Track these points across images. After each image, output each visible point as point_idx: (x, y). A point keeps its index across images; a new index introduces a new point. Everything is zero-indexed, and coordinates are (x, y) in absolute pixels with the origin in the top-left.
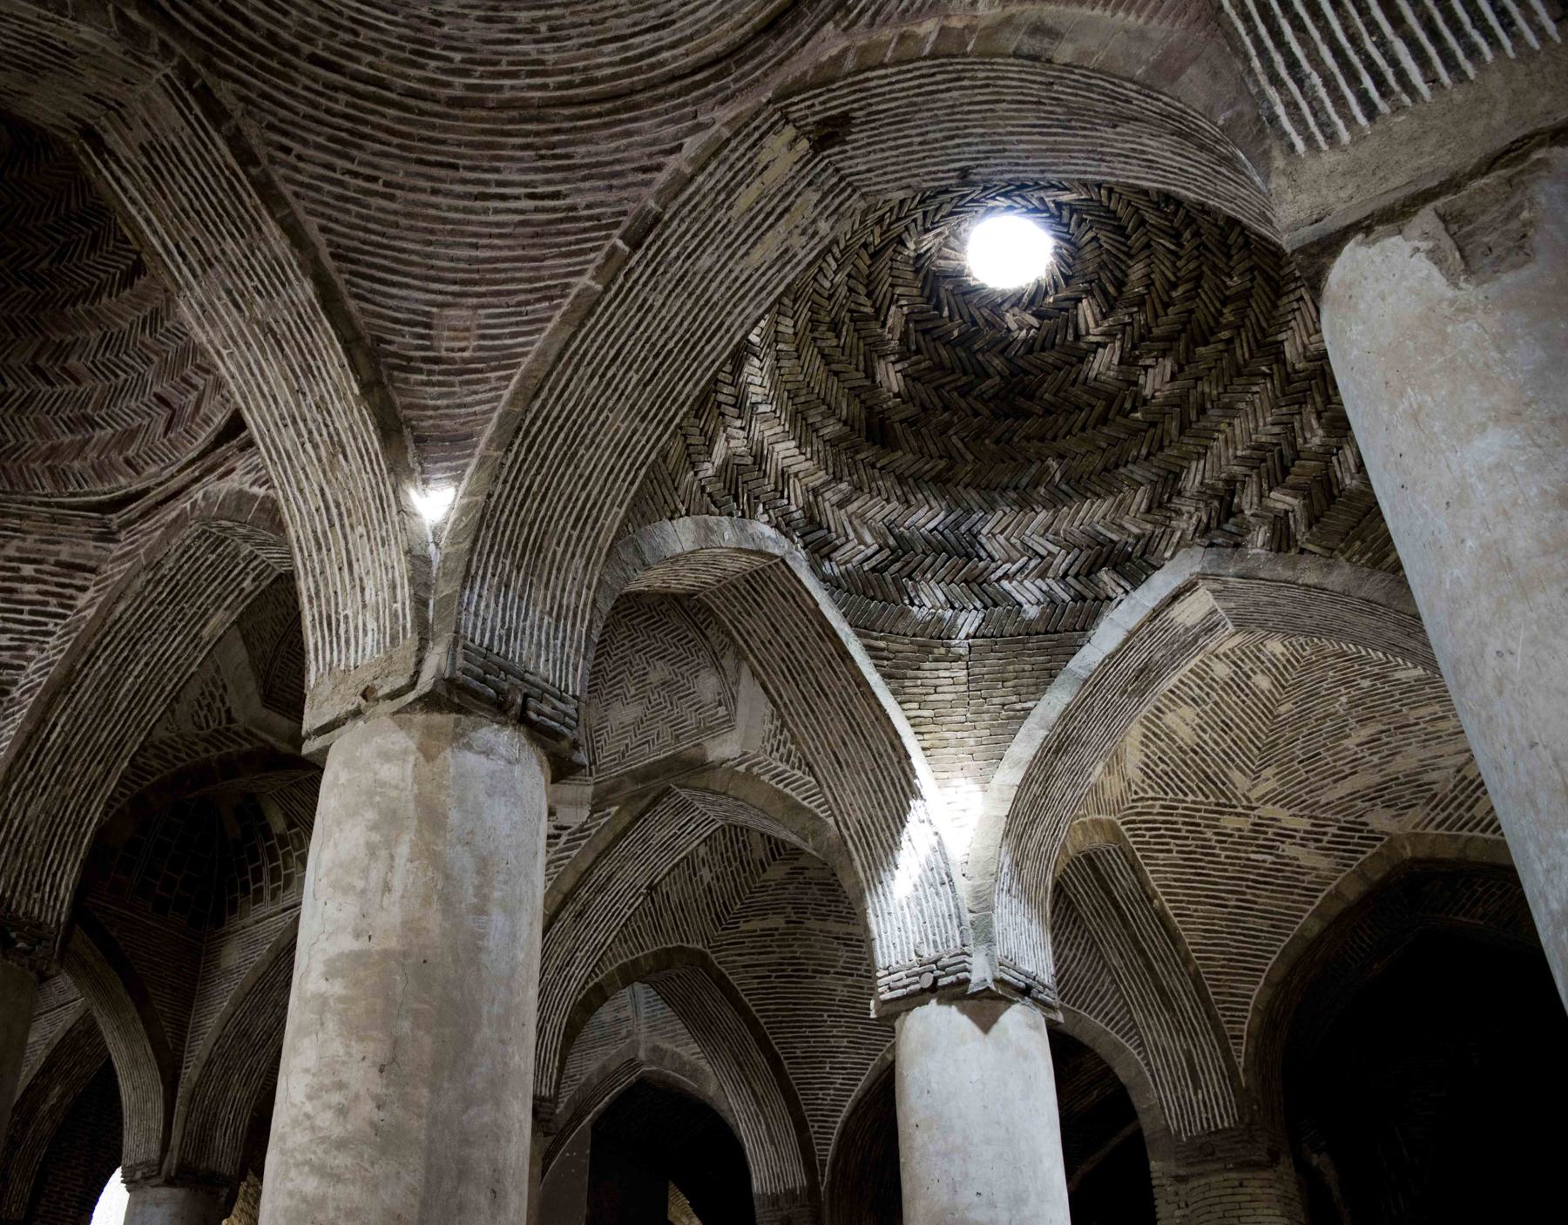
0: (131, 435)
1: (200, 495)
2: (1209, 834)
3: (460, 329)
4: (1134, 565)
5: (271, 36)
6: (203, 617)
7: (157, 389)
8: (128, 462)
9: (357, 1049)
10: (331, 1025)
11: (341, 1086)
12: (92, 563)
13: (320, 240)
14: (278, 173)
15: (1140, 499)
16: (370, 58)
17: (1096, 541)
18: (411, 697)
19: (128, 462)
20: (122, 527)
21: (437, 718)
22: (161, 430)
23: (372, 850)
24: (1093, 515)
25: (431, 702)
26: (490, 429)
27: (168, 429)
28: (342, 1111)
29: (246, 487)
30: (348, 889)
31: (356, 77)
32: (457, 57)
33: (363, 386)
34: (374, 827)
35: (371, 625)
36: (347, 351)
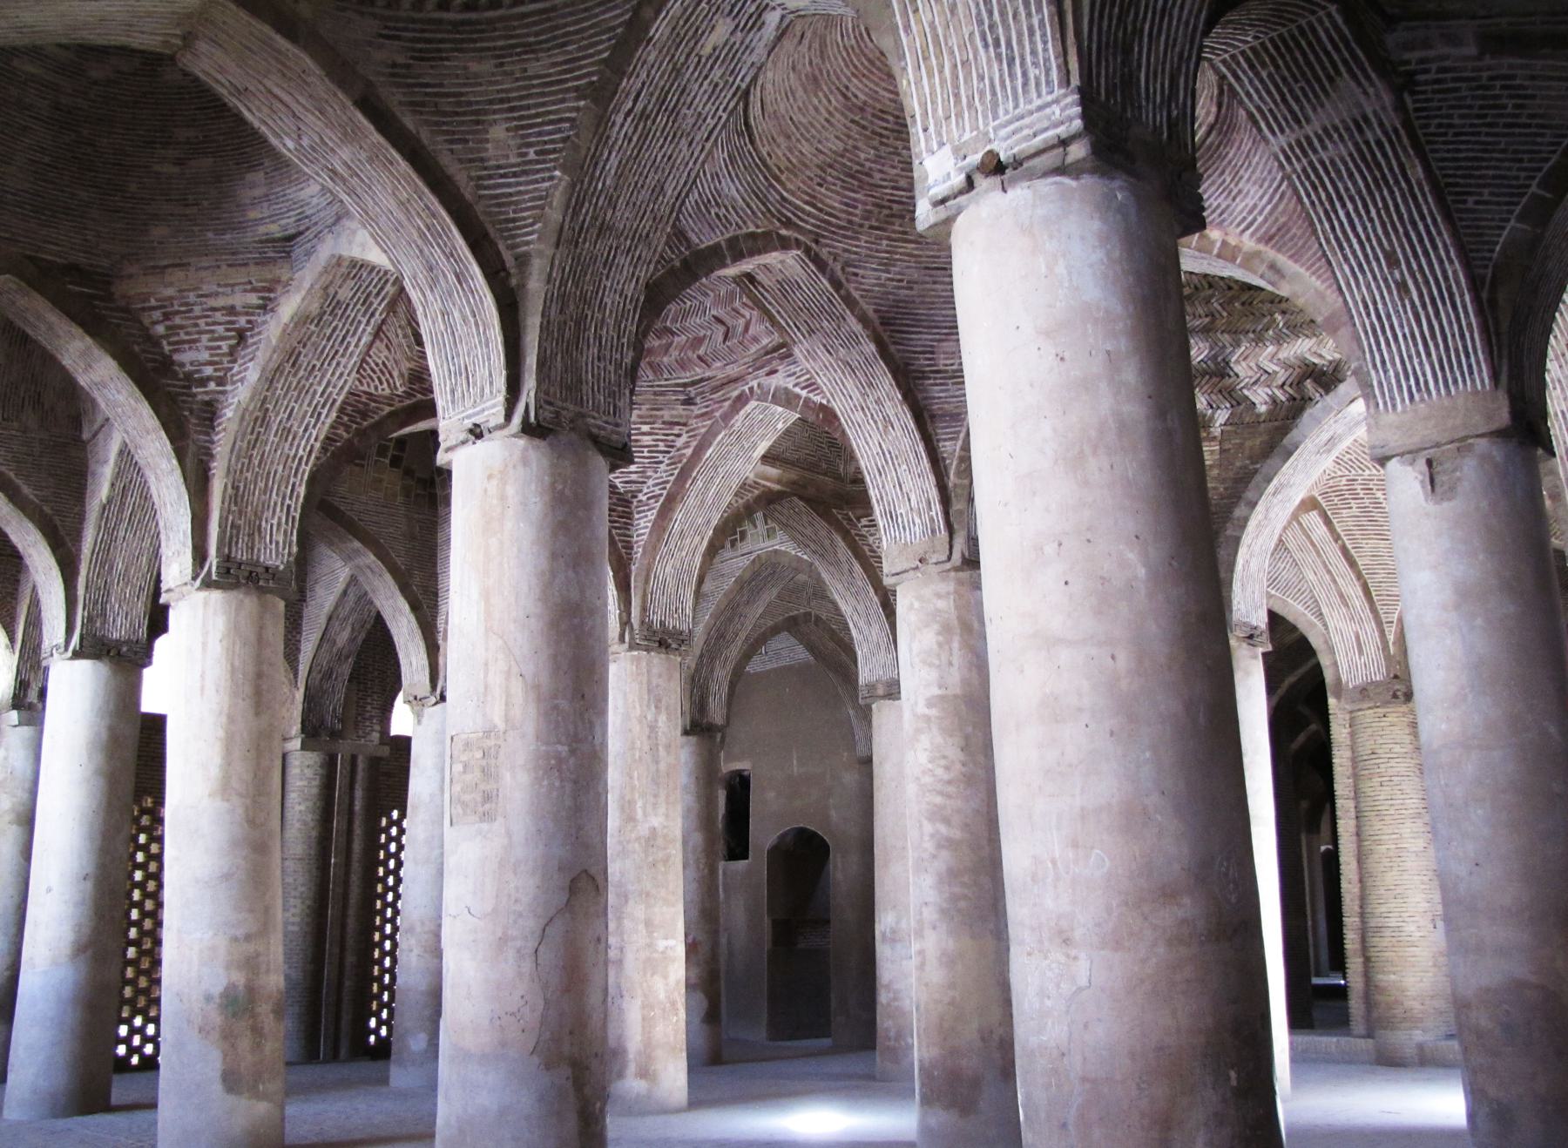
0: (699, 341)
1: (755, 383)
6: (754, 446)
7: (714, 312)
8: (699, 357)
10: (935, 730)
11: (944, 757)
12: (682, 420)
14: (851, 287)
18: (948, 566)
21: (961, 574)
22: (721, 339)
23: (940, 645)
27: (726, 338)
28: (947, 768)
29: (790, 386)
30: (931, 665)
33: (905, 396)
34: (939, 633)
35: (917, 521)
36: (895, 377)
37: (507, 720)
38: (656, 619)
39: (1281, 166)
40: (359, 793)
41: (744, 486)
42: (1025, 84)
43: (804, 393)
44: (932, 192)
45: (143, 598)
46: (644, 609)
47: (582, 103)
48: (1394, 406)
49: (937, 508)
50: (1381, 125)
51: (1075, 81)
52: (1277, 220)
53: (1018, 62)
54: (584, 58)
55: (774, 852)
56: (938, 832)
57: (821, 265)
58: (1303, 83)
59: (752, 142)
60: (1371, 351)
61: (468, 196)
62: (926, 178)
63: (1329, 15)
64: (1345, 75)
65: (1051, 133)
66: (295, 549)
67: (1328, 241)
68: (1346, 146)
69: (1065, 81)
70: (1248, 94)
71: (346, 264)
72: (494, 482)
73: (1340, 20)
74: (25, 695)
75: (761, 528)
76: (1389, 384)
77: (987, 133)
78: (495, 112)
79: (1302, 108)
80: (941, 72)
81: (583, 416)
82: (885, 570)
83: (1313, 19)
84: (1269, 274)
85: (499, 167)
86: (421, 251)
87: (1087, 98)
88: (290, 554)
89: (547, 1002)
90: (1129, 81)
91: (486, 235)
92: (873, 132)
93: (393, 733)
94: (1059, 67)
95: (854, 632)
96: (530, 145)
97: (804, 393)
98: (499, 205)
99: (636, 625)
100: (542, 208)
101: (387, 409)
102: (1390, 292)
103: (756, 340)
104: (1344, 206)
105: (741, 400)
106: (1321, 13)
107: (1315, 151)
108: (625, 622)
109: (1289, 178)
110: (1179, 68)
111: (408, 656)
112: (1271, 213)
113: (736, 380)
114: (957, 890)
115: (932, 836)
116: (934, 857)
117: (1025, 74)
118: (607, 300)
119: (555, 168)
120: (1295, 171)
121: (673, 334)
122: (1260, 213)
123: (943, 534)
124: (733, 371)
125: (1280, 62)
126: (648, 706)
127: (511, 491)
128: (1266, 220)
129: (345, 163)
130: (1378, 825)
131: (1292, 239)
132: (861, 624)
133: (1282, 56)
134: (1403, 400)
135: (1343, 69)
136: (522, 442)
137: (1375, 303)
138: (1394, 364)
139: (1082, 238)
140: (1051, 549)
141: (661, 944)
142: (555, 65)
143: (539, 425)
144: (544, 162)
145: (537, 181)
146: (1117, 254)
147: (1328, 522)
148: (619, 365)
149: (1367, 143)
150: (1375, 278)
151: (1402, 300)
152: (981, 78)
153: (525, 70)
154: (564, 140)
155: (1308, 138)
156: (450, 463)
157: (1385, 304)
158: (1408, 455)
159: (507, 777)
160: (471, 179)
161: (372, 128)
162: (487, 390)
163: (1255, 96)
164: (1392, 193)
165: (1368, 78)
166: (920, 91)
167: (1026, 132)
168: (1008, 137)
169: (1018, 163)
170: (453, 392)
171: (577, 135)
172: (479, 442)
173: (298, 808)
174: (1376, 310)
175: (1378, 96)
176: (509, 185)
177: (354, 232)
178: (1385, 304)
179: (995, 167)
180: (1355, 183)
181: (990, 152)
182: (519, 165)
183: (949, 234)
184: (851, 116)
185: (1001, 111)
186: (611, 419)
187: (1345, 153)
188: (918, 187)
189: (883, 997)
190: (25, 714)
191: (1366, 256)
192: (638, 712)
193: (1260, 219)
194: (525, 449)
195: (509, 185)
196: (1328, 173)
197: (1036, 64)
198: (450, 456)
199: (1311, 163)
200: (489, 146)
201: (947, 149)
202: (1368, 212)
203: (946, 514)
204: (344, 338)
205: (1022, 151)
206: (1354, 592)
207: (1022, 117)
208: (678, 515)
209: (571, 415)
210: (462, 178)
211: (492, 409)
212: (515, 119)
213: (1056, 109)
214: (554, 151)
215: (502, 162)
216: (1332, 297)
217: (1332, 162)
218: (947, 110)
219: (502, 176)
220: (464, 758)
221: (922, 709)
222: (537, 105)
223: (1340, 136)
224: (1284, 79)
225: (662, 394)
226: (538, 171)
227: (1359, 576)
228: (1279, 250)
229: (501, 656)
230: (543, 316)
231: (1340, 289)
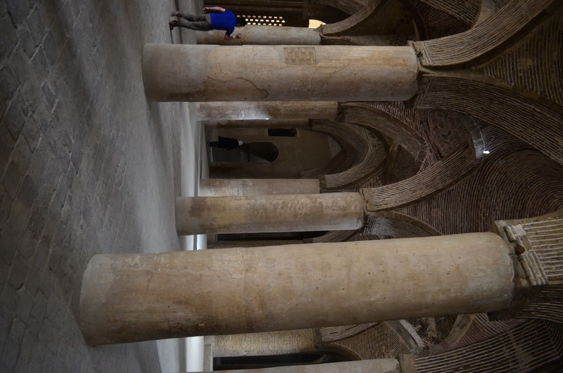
0: (442, 126)
1: (427, 145)
2: (382, 343)
3: (437, 213)
4: (422, 332)
5: (485, 182)
6: (405, 144)
8: (437, 126)
9: (308, 209)
10: (312, 204)
11: (303, 207)
13: (451, 188)
14: (462, 181)
15: (435, 335)
16: (485, 198)
17: (427, 325)
18: (365, 210)
19: (437, 126)
20: (424, 126)
21: (363, 214)
23: (339, 207)
24: (432, 324)
25: (364, 213)
26: (417, 219)
27: (443, 135)
28: (299, 208)
30: (333, 204)
31: (481, 197)
32: (487, 215)
33: (423, 197)
35: (381, 200)
36: (429, 194)
37: (320, 67)
38: (348, 111)
39: (502, 333)
40: (290, 9)
41: (391, 139)
42: (549, 264)
43: (424, 162)
44: (509, 227)
46: (351, 107)
47: (539, 93)
48: (416, 364)
49: (385, 207)
50: (515, 369)
51: (551, 283)
52: (481, 328)
53: (558, 261)
54: (556, 95)
55: (270, 145)
56: (279, 205)
57: (470, 172)
58: (531, 344)
59: (517, 151)
60: (435, 357)
61: (506, 51)
62: (514, 225)
63: (556, 356)
64: (534, 359)
65: (531, 273)
67: (474, 346)
68: (508, 356)
69: (550, 279)
70: (528, 325)
71: (478, 5)
72: (402, 62)
73: (554, 359)
75: (376, 143)
76: (424, 363)
77: (531, 248)
78: (537, 61)
79: (522, 343)
80: (554, 232)
81: (424, 93)
82: (365, 189)
83: (555, 350)
84: (462, 324)
85: (516, 63)
86: (486, 34)
87: (543, 287)
89: (225, 82)
90: (547, 299)
91: (491, 58)
92: (517, 191)
93: (311, 21)
94: (556, 277)
95: (342, 173)
96: (524, 75)
97: (424, 162)
98: (502, 62)
99: (346, 104)
100: (500, 78)
101: (423, 19)
102: (455, 365)
103: (442, 146)
104: (486, 353)
105: (422, 140)
106: (557, 353)
107: (506, 345)
109: (496, 336)
110: (549, 315)
111: (336, 26)
112: (483, 326)
113: (429, 138)
114: (260, 211)
115: (278, 203)
116: (271, 204)
117: (553, 264)
118: (465, 101)
119: (515, 83)
120: (499, 338)
121: (445, 118)
122: (483, 322)
123: (376, 209)
124: (432, 137)
125: (539, 337)
127: (399, 68)
128: (481, 324)
129: (520, 6)
130: (277, 336)
131: (474, 333)
132: (344, 176)
133: (542, 338)
134: (418, 367)
135: (536, 358)
136: (416, 71)
137: (452, 360)
138: (430, 365)
139: (491, 282)
140: (381, 267)
141: (243, 112)
142: (554, 83)
143: (422, 77)
144: (517, 79)
145: (510, 76)
146: (485, 294)
147: (373, 327)
148: (441, 105)
149: (508, 363)
150: (460, 361)
151: (452, 369)
152: (552, 247)
153: (552, 72)
154: (525, 87)
155: (511, 343)
156: (409, 45)
157: (451, 363)
158: (400, 368)
159: (300, 68)
160: (513, 52)
161: (534, 16)
162: (434, 59)
163: (527, 327)
164: (490, 369)
165: (532, 366)
166: (547, 223)
167: (532, 263)
168: (530, 257)
169: (520, 260)
170: (434, 46)
171: (527, 91)
172: (415, 56)
174: (449, 360)
175: (524, 369)
176: (509, 66)
177: (490, 8)
178: (451, 363)
179: (518, 251)
180: (494, 357)
181: (524, 250)
182: (517, 70)
183: (493, 232)
184: (524, 184)
185: (539, 254)
186: (422, 102)
187: (505, 355)
188: (510, 221)
189: (226, 181)
191: (468, 359)
193: (481, 322)
194: (413, 73)
195: (509, 66)
196: (498, 349)
197: (557, 268)
198: (411, 45)
199: (502, 343)
200: (525, 59)
201: (525, 233)
202: (483, 361)
203: (383, 210)
204: (451, 4)
205: (524, 262)
206: (350, 333)
207: (537, 262)
208: (383, 119)
209: (424, 88)
210: (514, 49)
211: (427, 61)
212: (534, 69)
213: (540, 275)
214: (521, 83)
215: (518, 64)
216: (453, 345)
217: (502, 351)
218: (540, 233)
219: (513, 64)
220: (307, 52)
221: (319, 200)
222: (539, 76)
223: (511, 354)
224: (533, 338)
225: (424, 113)
226: (514, 77)
227: (355, 335)
228: (470, 327)
229: (342, 65)
230: (461, 79)
231: (457, 349)
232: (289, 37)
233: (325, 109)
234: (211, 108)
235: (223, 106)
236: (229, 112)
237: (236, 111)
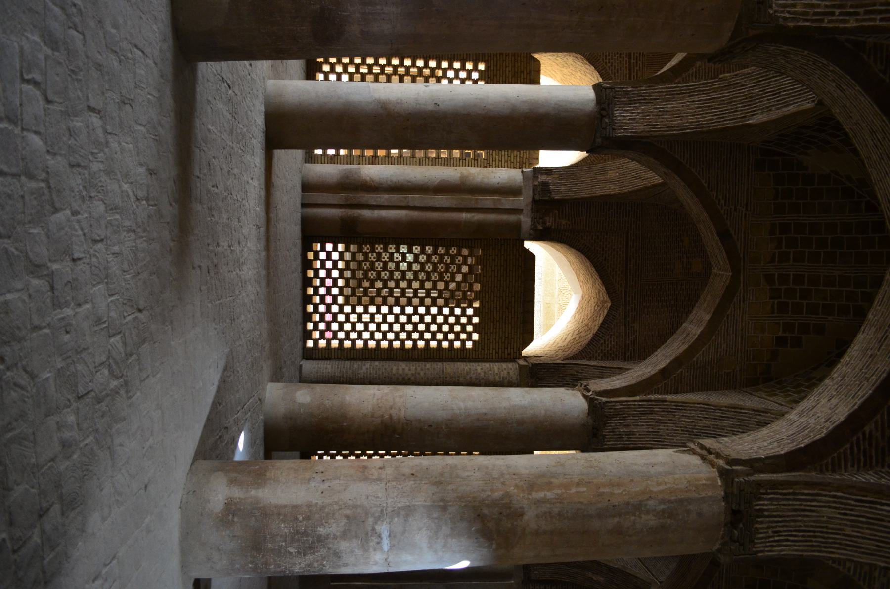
45: (647, 129)
46: (774, 485)
66: (791, 24)
74: (542, 174)
88: (785, 19)
108: (754, 464)
126: (663, 501)
141: (383, 529)
173: (479, 368)
190: (531, 175)
192: (655, 489)
232: (505, 404)
233: (681, 501)
234: (266, 513)
235: (309, 505)
236: (333, 528)
237: (359, 523)
